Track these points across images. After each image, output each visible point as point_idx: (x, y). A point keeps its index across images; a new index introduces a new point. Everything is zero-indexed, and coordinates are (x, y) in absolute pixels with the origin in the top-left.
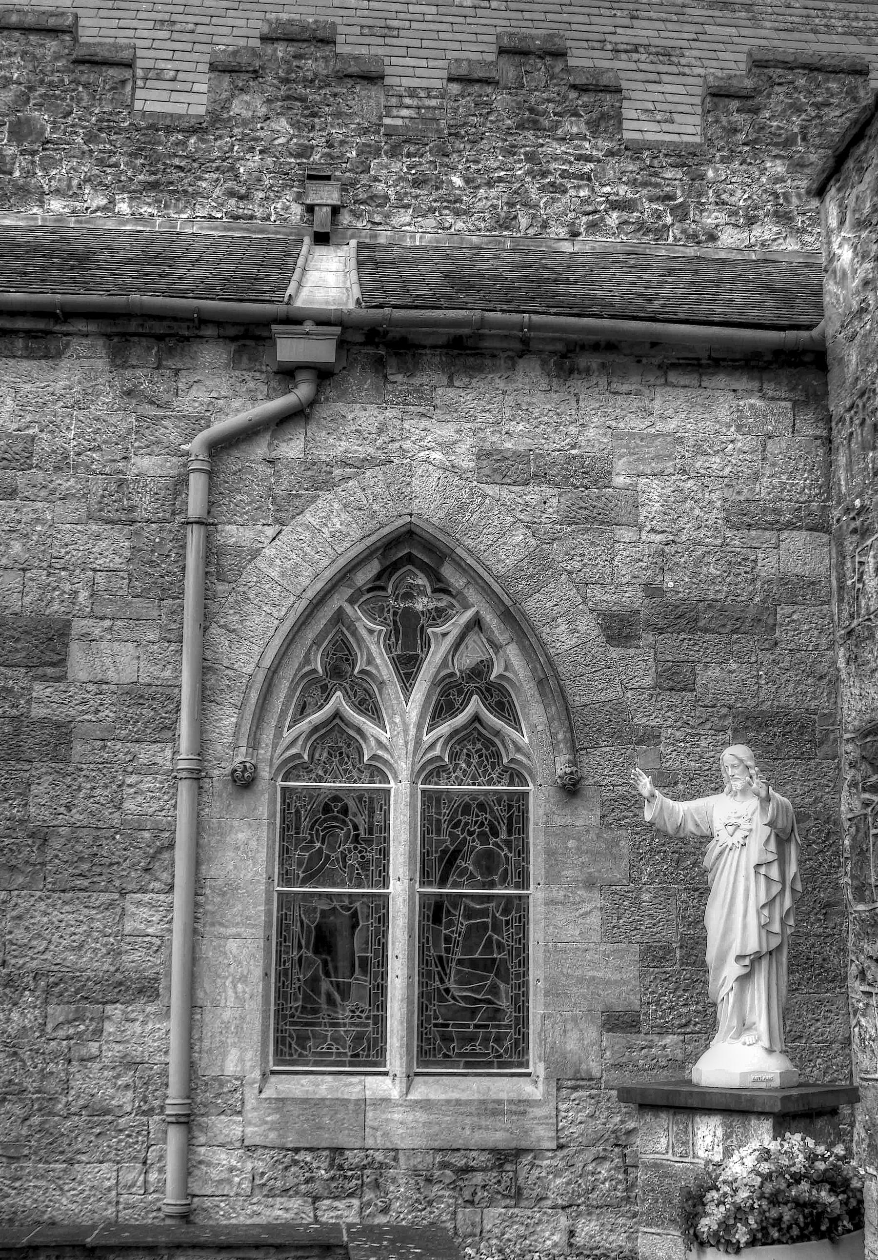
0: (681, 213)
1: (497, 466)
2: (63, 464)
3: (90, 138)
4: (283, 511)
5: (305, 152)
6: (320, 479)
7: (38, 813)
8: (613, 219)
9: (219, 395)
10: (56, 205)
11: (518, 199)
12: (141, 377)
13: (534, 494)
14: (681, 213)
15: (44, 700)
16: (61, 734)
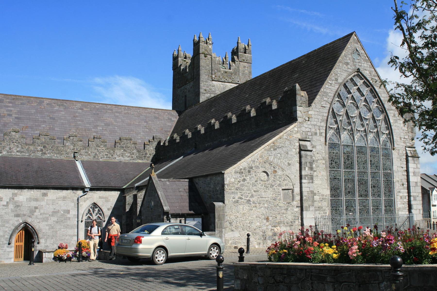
0: (112, 156)
1: (100, 198)
2: (69, 198)
3: (52, 148)
4: (85, 201)
5: (74, 149)
6: (87, 199)
7: (68, 224)
8: (105, 156)
9: (80, 193)
10: (48, 155)
11: (96, 154)
12: (75, 191)
13: (103, 199)
14: (112, 156)
15: (68, 216)
16: (70, 218)
